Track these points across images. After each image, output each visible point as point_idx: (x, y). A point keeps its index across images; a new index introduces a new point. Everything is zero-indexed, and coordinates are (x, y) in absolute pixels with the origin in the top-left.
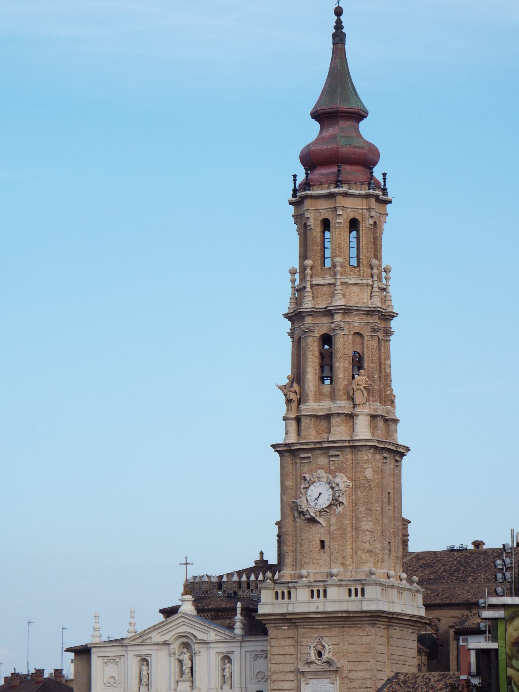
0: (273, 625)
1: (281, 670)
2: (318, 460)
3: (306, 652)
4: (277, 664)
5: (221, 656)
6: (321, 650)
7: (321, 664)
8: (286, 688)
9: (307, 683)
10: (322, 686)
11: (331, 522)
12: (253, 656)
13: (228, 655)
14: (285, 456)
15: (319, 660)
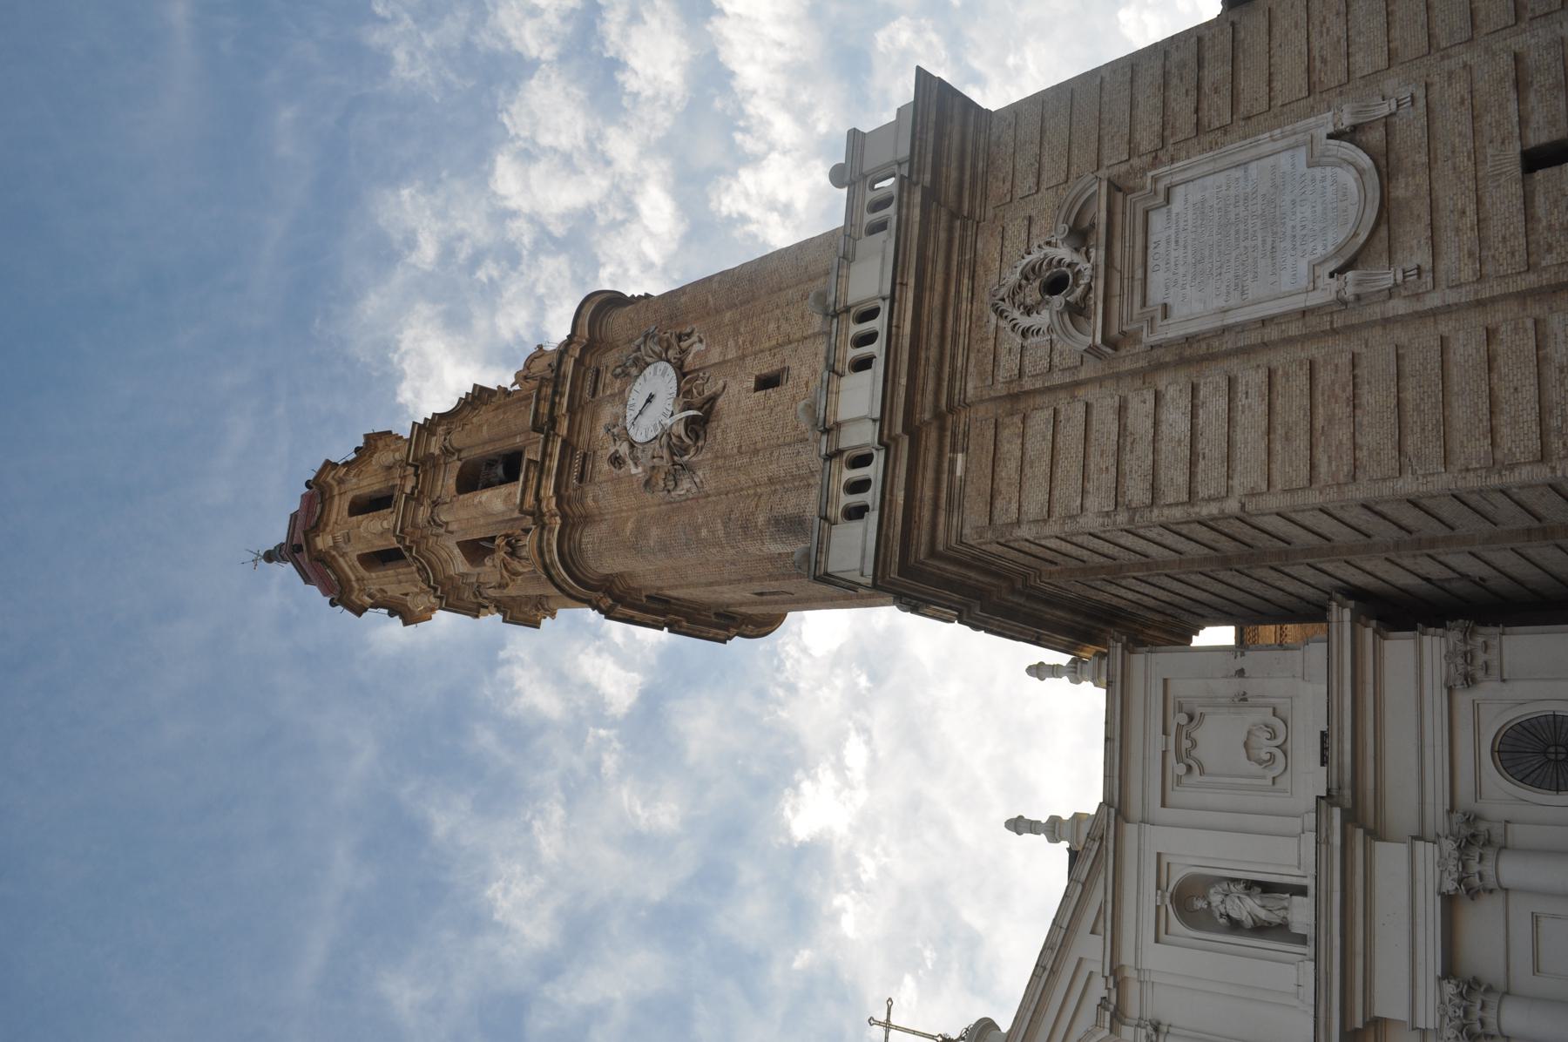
0: (942, 519)
1: (1112, 461)
2: (600, 437)
3: (1043, 352)
4: (1090, 487)
5: (1176, 925)
6: (1037, 284)
7: (1089, 265)
8: (1183, 426)
9: (1159, 315)
10: (1177, 242)
11: (717, 361)
12: (1181, 769)
13: (1171, 888)
14: (580, 539)
15: (1076, 284)
